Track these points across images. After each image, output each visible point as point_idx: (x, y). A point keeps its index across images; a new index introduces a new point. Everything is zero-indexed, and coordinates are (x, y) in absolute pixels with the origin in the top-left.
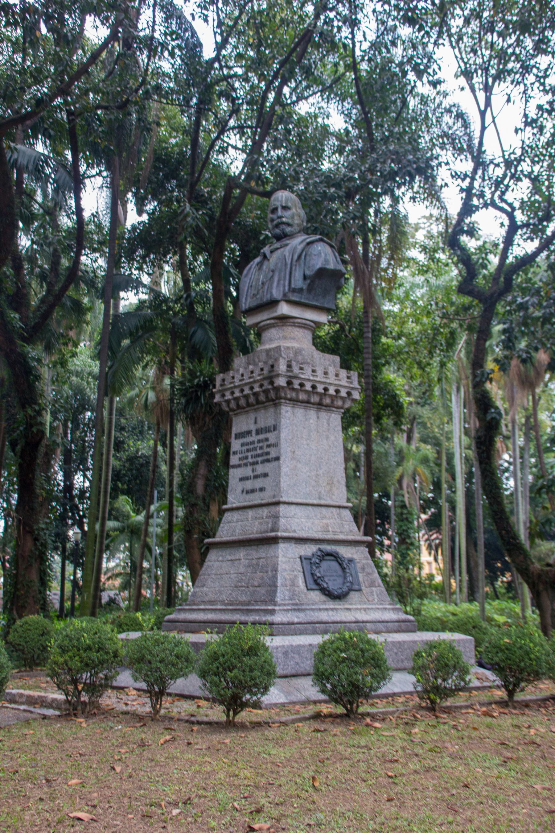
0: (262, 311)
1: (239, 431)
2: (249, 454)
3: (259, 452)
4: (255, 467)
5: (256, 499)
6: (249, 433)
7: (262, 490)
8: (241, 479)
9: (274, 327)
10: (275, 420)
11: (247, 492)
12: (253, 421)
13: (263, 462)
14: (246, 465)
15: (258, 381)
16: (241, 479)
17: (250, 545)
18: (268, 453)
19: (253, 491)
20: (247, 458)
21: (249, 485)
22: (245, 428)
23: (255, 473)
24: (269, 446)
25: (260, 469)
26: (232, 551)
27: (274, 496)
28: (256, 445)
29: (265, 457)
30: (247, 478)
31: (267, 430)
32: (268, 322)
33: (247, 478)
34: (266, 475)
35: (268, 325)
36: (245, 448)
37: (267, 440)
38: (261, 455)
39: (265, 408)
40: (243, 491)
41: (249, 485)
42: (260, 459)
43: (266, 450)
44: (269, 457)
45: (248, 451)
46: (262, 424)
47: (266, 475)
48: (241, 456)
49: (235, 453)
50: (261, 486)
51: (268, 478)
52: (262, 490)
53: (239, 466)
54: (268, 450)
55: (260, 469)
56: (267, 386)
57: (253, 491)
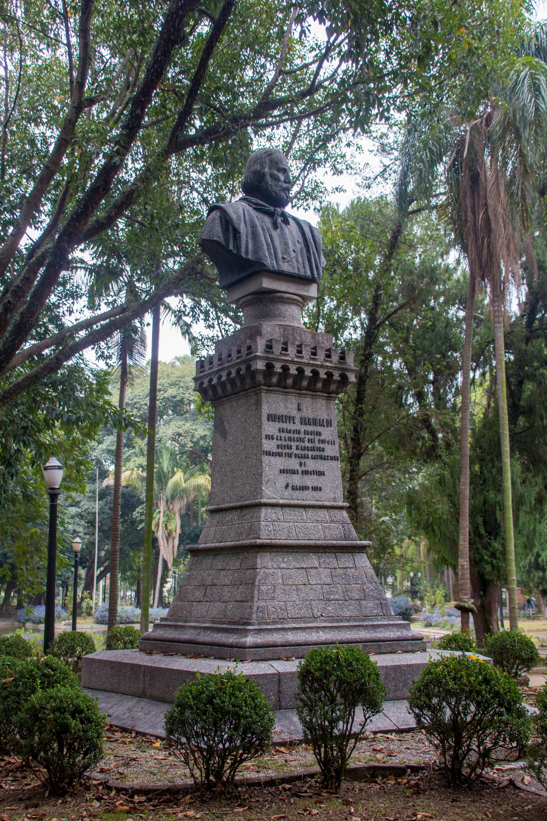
0: (279, 279)
1: (272, 412)
2: (294, 444)
3: (307, 444)
4: (303, 461)
5: (309, 498)
6: (290, 419)
7: (315, 489)
8: (282, 471)
9: (297, 305)
10: (328, 415)
11: (293, 488)
12: (295, 406)
13: (314, 458)
14: (290, 456)
15: (327, 367)
16: (282, 471)
17: (326, 552)
18: (319, 449)
19: (304, 488)
20: (290, 448)
21: (296, 480)
22: (281, 411)
23: (303, 468)
24: (323, 442)
25: (311, 465)
26: (299, 556)
27: (335, 500)
28: (302, 436)
29: (318, 453)
30: (293, 472)
31: (314, 422)
32: (296, 297)
33: (293, 472)
34: (321, 474)
35: (294, 300)
36: (287, 435)
37: (319, 434)
38: (313, 449)
39: (314, 397)
40: (287, 486)
41: (296, 480)
42: (310, 453)
43: (317, 445)
44: (325, 454)
45: (290, 439)
46: (308, 413)
47: (321, 474)
48: (280, 443)
49: (268, 437)
50: (315, 485)
51: (322, 478)
52: (315, 489)
53: (280, 455)
54: (321, 445)
55: (311, 465)
56: (336, 376)
57: (304, 488)
